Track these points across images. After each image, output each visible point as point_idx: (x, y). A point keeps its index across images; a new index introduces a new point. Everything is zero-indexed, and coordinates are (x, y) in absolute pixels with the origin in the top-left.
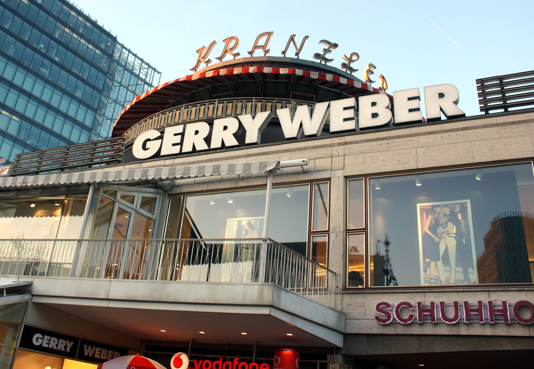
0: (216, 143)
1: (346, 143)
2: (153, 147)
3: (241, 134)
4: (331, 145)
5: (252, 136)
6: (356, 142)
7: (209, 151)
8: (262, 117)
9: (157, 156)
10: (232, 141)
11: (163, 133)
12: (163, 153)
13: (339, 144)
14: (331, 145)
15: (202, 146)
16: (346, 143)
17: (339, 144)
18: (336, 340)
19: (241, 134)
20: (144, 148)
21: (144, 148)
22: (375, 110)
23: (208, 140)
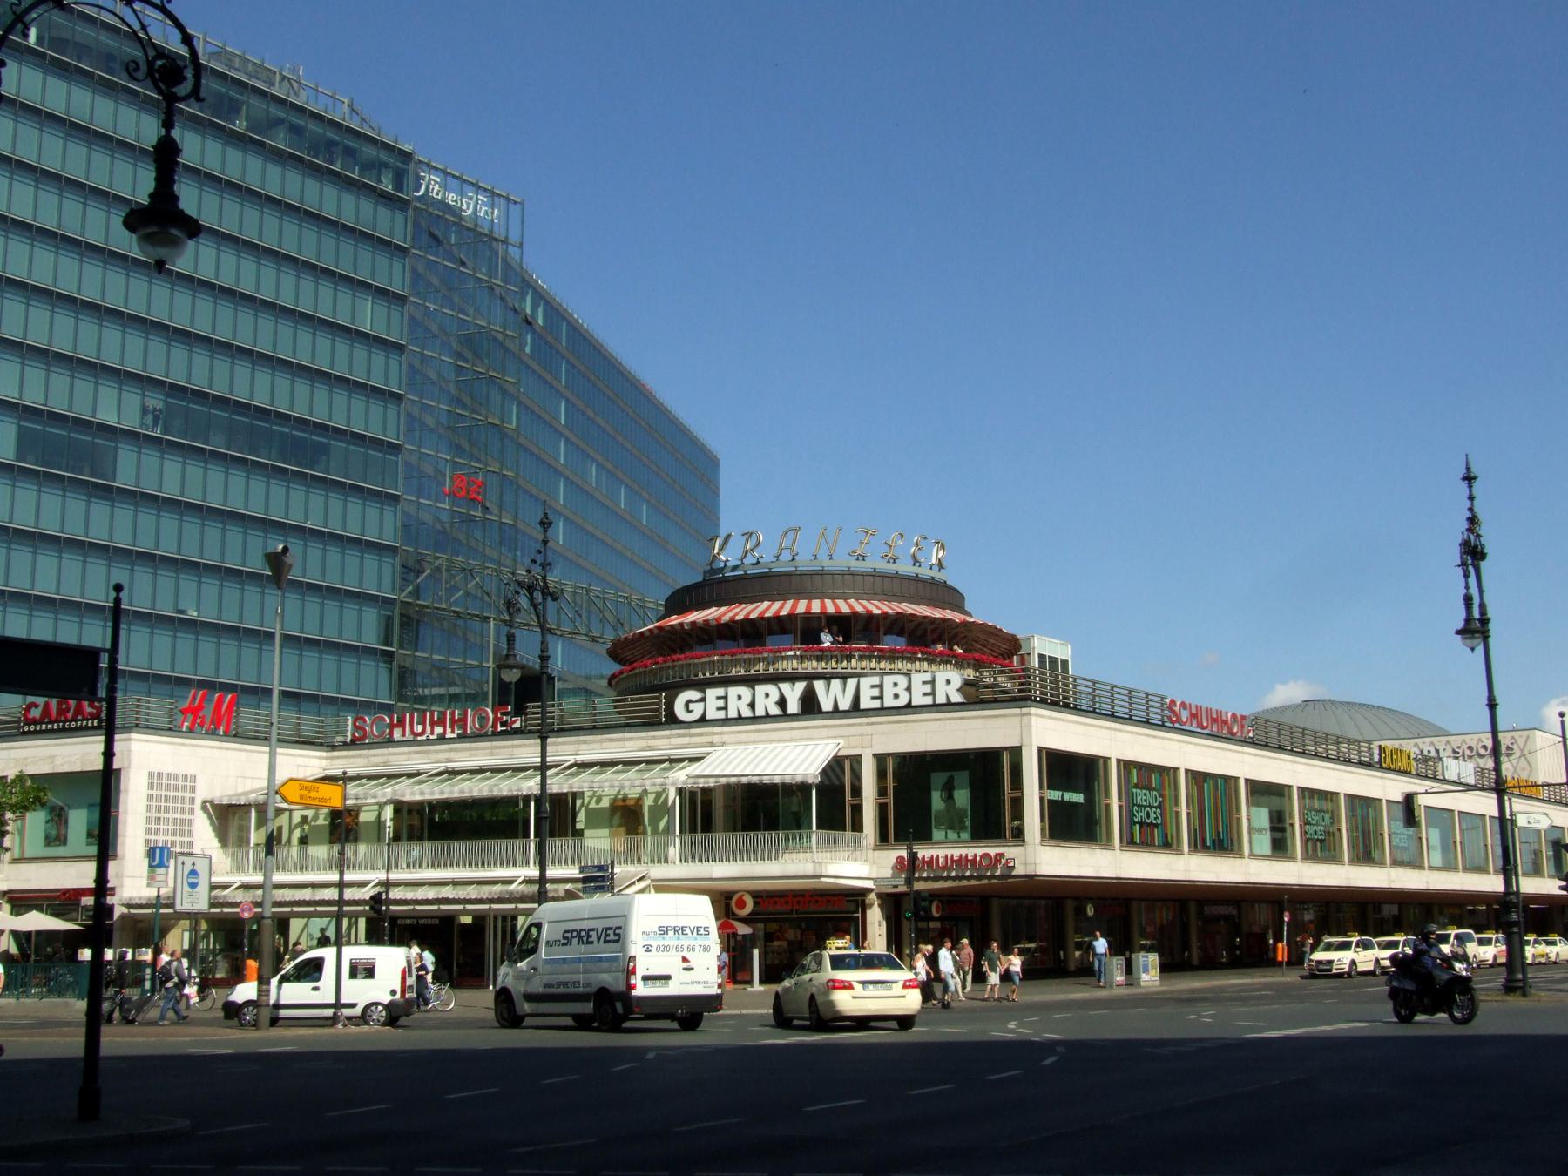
0: (760, 712)
1: (873, 724)
2: (697, 710)
3: (782, 703)
4: (860, 724)
5: (793, 707)
6: (881, 723)
7: (754, 719)
8: (800, 686)
9: (703, 720)
10: (775, 710)
11: (705, 693)
12: (708, 718)
13: (868, 724)
14: (860, 724)
15: (746, 713)
16: (873, 724)
17: (868, 724)
18: (869, 884)
19: (782, 703)
20: (689, 711)
21: (689, 711)
22: (896, 690)
23: (752, 705)
